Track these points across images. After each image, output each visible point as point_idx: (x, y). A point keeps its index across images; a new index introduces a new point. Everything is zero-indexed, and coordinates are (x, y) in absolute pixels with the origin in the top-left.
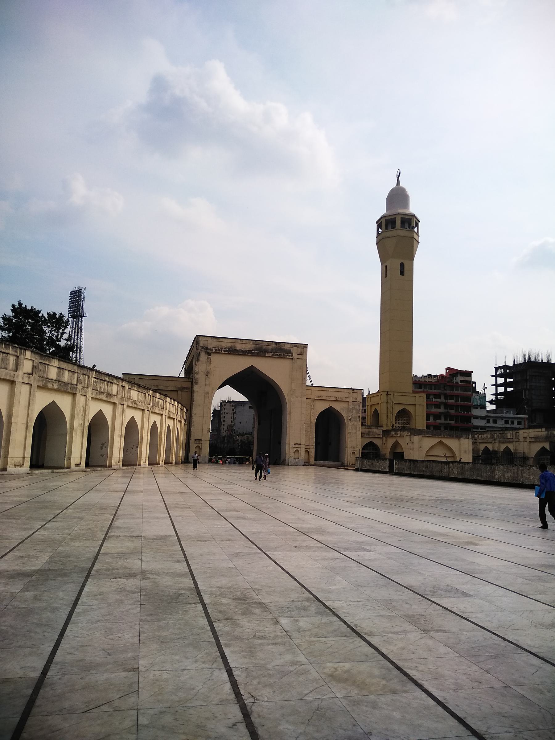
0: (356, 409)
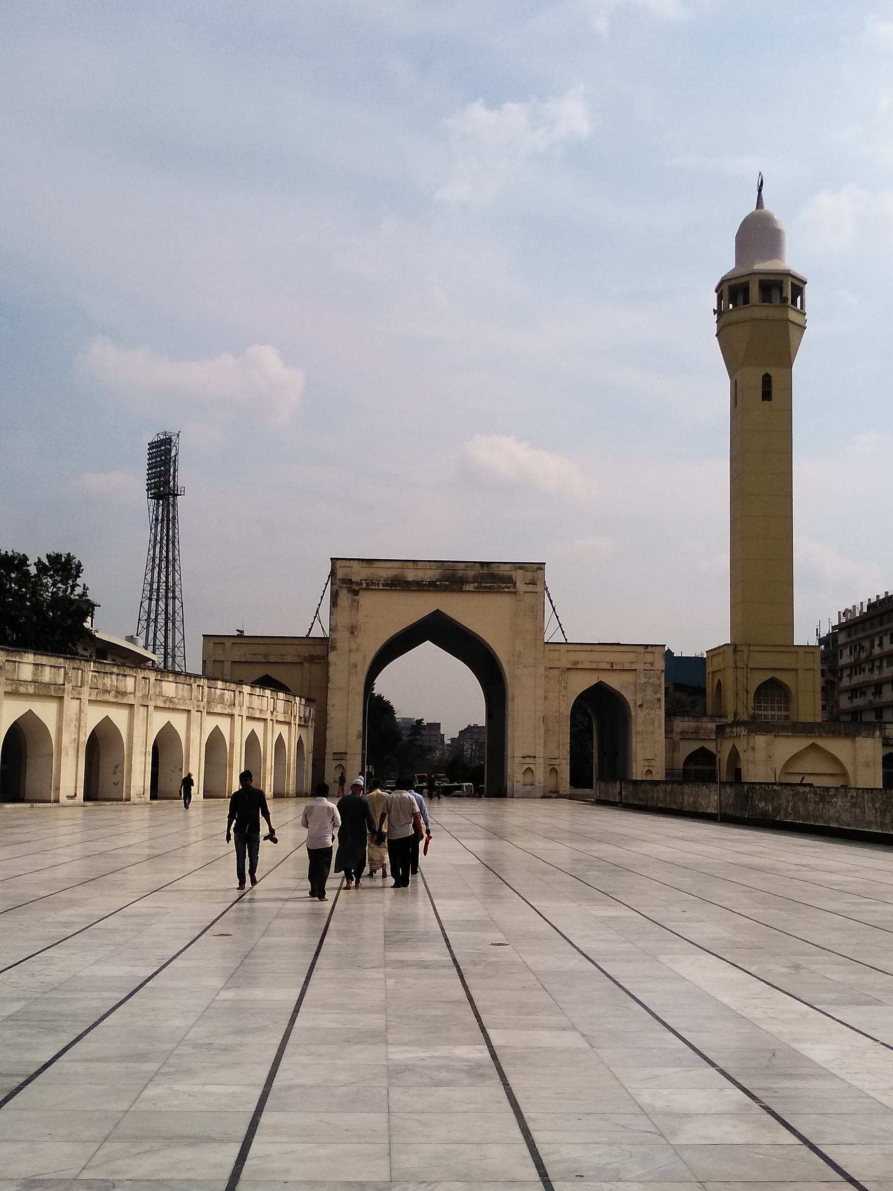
0: (653, 684)
